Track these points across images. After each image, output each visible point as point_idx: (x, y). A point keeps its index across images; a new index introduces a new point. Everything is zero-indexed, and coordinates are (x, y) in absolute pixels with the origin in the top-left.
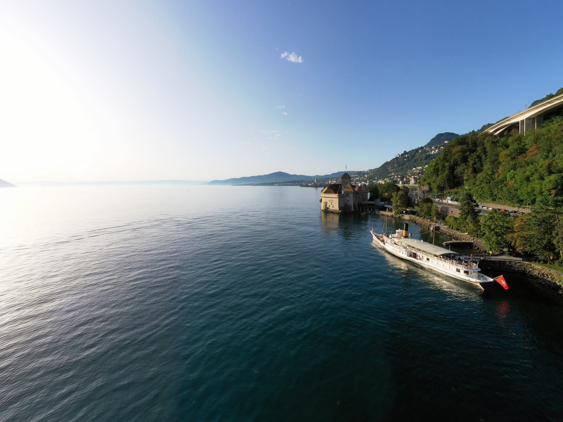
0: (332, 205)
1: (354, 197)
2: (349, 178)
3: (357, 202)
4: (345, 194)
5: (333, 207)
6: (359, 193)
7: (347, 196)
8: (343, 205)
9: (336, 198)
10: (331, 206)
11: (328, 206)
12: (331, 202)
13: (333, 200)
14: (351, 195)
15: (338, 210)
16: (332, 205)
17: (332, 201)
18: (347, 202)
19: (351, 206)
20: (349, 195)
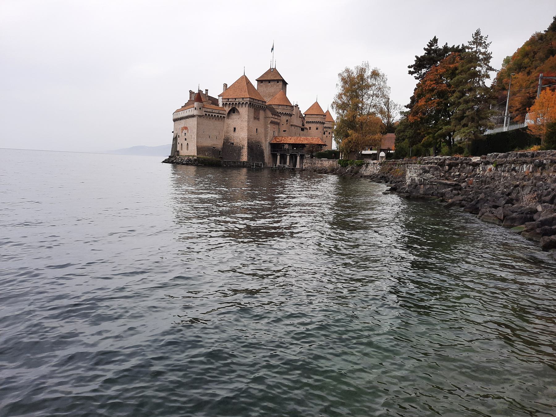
0: (186, 142)
1: (256, 118)
2: (278, 81)
3: (269, 140)
4: (227, 109)
5: (187, 150)
6: (279, 111)
7: (234, 116)
8: (219, 144)
9: (193, 116)
10: (185, 143)
11: (179, 148)
12: (185, 131)
13: (188, 126)
14: (244, 111)
15: (196, 154)
16: (186, 142)
17: (186, 128)
18: (232, 134)
19: (240, 149)
20: (238, 112)
